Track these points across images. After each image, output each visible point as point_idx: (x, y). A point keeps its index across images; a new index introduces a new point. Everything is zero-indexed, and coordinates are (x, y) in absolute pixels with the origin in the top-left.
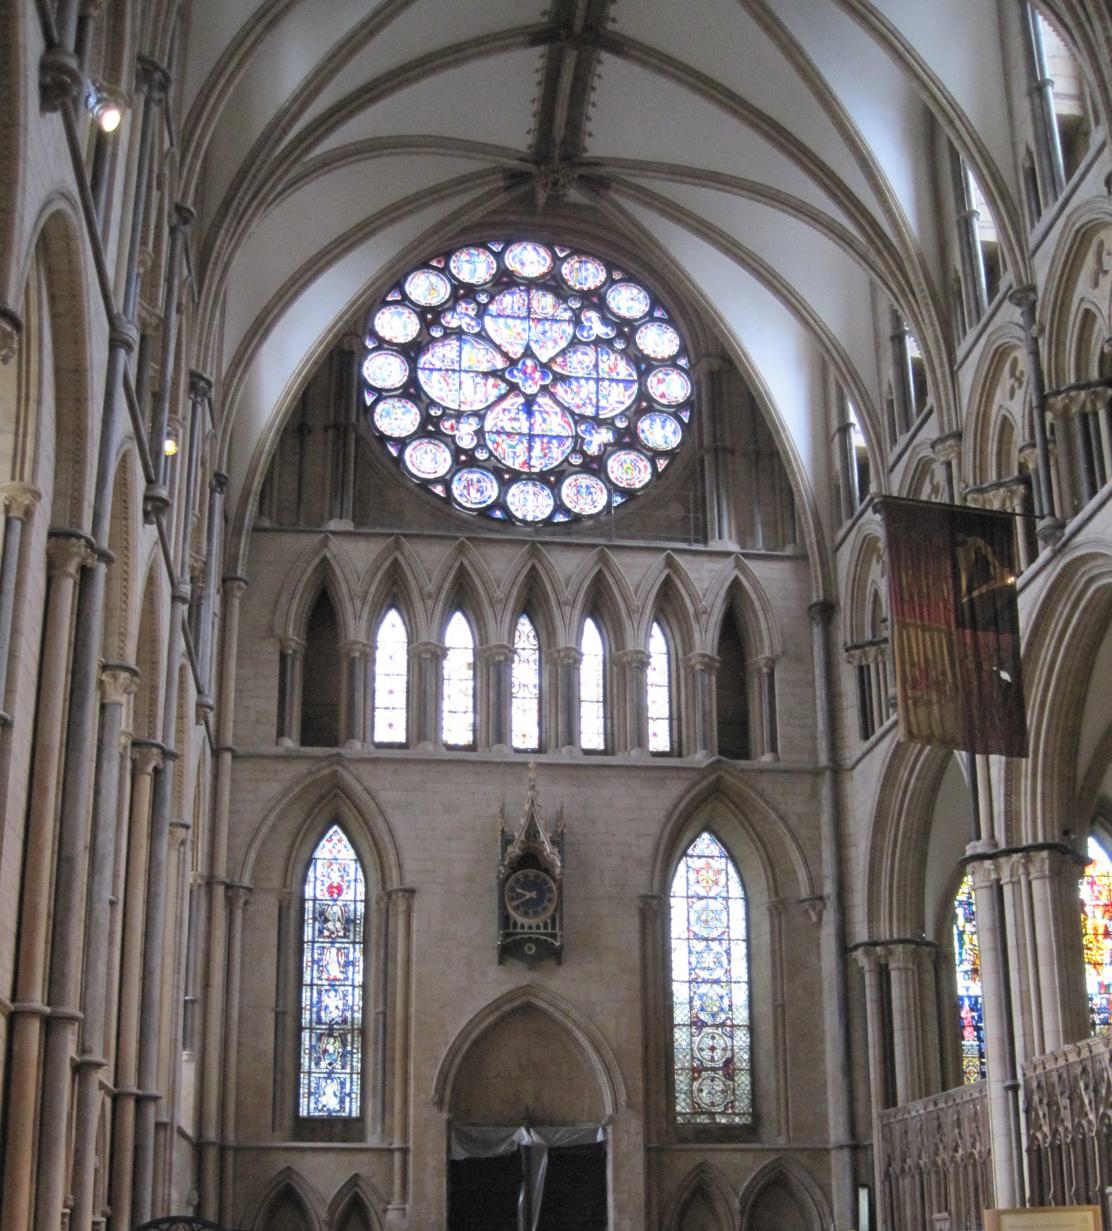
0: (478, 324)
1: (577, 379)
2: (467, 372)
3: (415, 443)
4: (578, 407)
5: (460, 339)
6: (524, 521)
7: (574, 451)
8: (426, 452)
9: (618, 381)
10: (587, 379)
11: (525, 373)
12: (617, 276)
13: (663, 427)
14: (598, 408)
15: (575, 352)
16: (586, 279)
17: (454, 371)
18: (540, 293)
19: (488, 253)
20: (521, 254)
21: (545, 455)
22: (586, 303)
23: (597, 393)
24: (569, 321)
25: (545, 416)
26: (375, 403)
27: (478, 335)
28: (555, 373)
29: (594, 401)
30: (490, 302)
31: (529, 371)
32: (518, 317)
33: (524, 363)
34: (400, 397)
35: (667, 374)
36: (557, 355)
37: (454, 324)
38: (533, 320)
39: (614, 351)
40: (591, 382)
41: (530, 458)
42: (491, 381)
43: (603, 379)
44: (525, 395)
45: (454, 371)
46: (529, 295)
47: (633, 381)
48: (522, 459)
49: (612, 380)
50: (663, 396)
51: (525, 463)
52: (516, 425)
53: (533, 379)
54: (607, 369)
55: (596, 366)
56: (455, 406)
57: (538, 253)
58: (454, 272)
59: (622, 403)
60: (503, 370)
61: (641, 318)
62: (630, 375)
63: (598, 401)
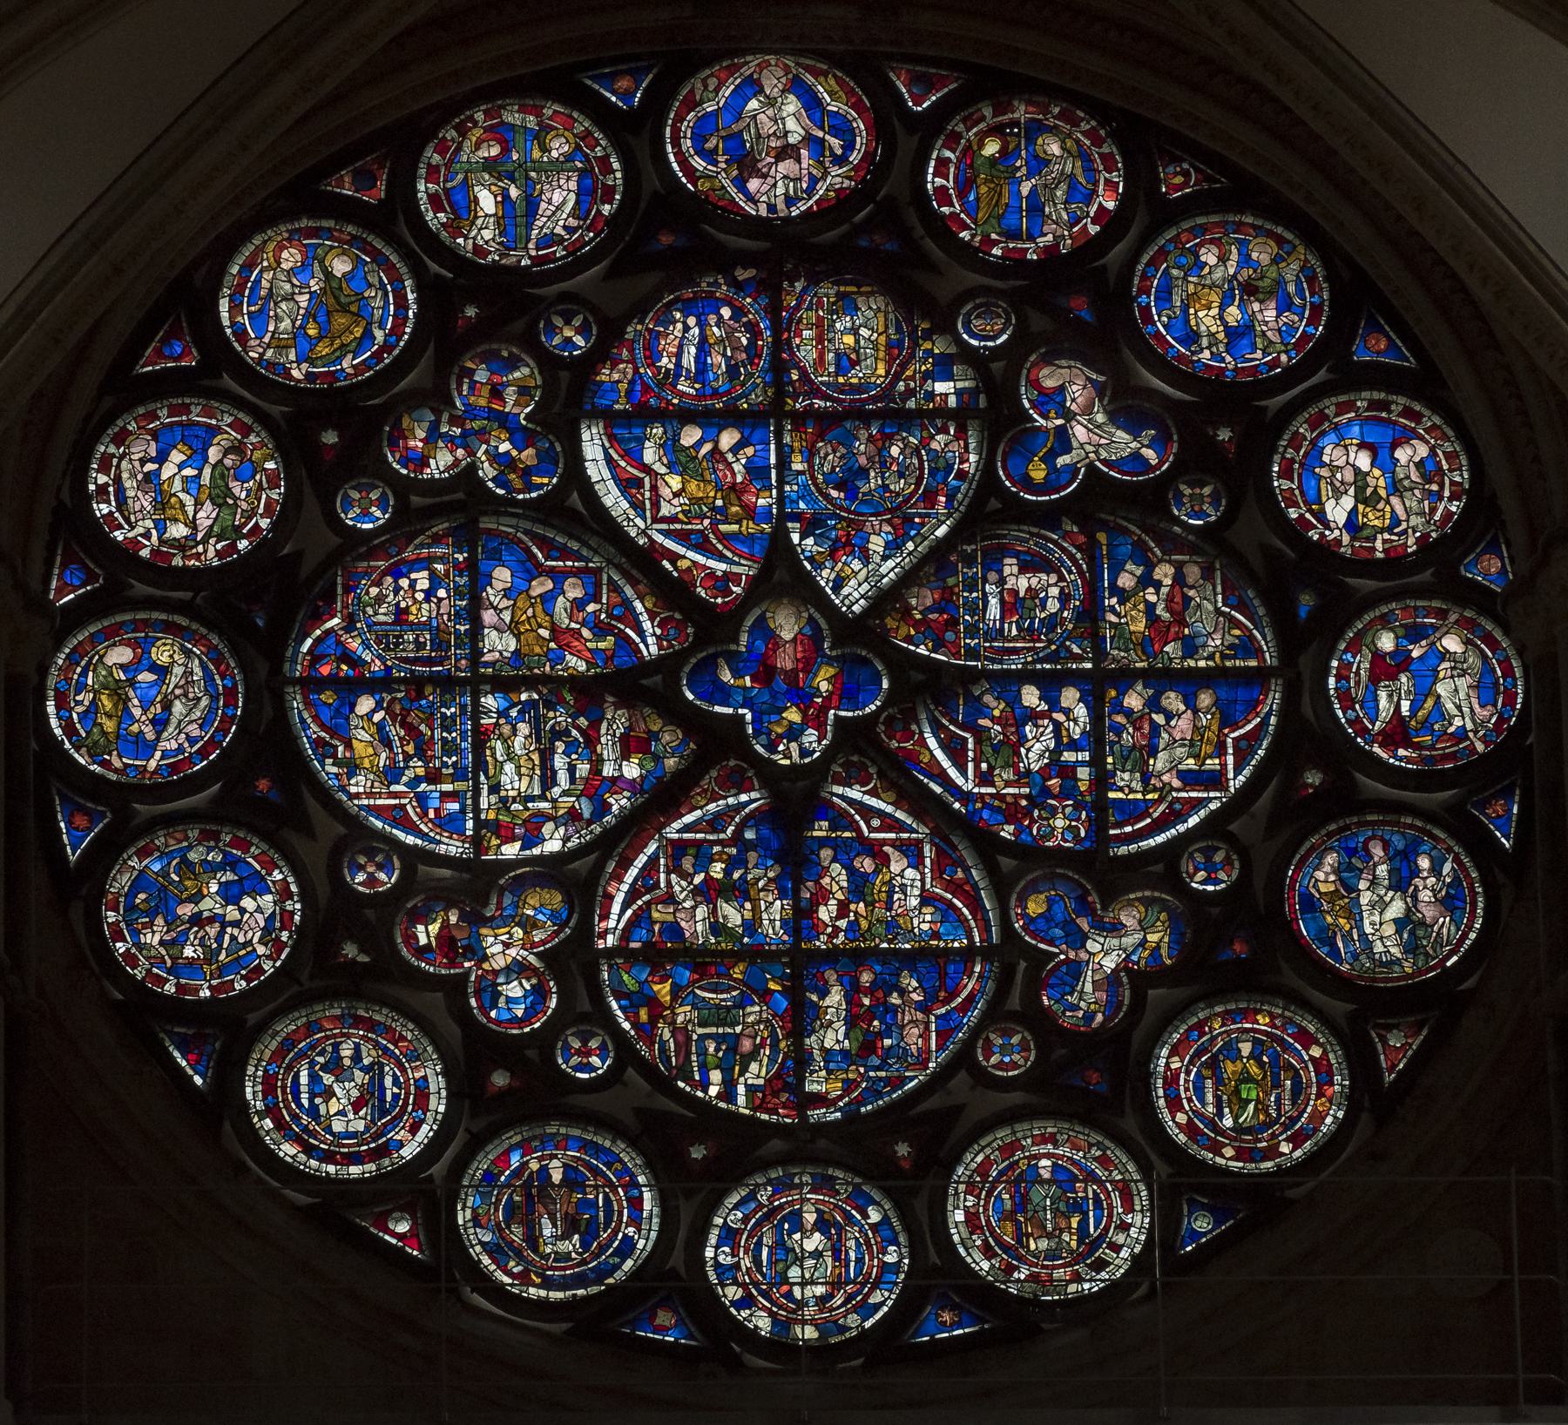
0: (546, 461)
1: (1008, 684)
2: (503, 685)
3: (286, 1027)
4: (1012, 812)
5: (466, 536)
6: (780, 1347)
7: (994, 1016)
8: (335, 1066)
9: (1189, 682)
10: (1051, 685)
11: (765, 673)
12: (1176, 182)
13: (1402, 881)
14: (1098, 826)
15: (993, 561)
16: (1035, 207)
17: (447, 684)
18: (828, 291)
19: (583, 124)
20: (735, 107)
21: (868, 1047)
22: (1039, 322)
23: (1096, 739)
24: (961, 416)
25: (867, 865)
26: (105, 854)
27: (550, 510)
28: (901, 663)
29: (1083, 773)
30: (600, 354)
31: (785, 661)
32: (730, 417)
33: (763, 630)
34: (210, 821)
35: (1415, 633)
36: (908, 579)
37: (441, 462)
38: (800, 419)
39: (1172, 545)
40: (1069, 696)
41: (802, 1060)
42: (616, 722)
43: (1125, 678)
44: (769, 775)
45: (447, 684)
46: (774, 310)
47: (1260, 677)
48: (756, 1073)
49: (1161, 679)
50: (1397, 733)
51: (775, 1084)
52: (732, 915)
53: (802, 697)
54: (1140, 626)
55: (1091, 614)
56: (452, 847)
57: (812, 104)
58: (435, 219)
59: (1216, 780)
60: (667, 665)
61: (1292, 375)
62: (1246, 647)
63: (1102, 780)
